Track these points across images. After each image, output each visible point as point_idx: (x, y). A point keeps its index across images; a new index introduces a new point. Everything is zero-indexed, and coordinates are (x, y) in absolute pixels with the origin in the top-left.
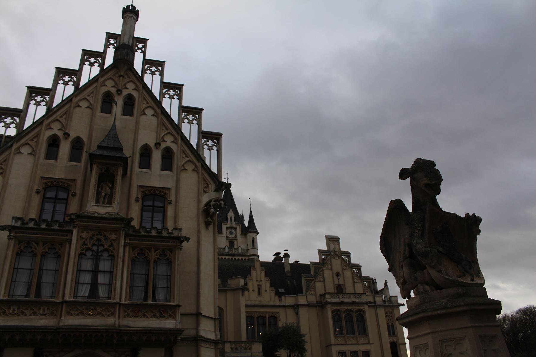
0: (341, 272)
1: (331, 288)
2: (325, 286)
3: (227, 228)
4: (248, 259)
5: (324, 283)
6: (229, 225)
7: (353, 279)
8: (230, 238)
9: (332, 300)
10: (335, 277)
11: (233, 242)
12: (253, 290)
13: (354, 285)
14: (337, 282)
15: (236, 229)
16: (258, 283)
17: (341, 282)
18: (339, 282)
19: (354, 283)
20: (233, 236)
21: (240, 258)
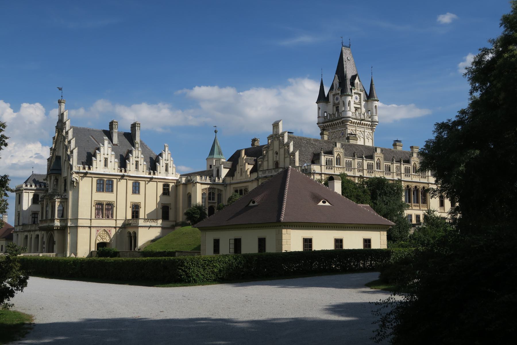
0: (278, 151)
1: (271, 165)
2: (268, 164)
3: (334, 95)
4: (342, 122)
5: (268, 162)
6: (334, 92)
7: (285, 154)
8: (336, 103)
9: (263, 176)
10: (275, 155)
11: (338, 107)
12: (239, 173)
13: (284, 160)
14: (275, 160)
15: (339, 93)
16: (241, 168)
17: (277, 160)
18: (276, 159)
19: (285, 158)
20: (338, 102)
21: (336, 122)
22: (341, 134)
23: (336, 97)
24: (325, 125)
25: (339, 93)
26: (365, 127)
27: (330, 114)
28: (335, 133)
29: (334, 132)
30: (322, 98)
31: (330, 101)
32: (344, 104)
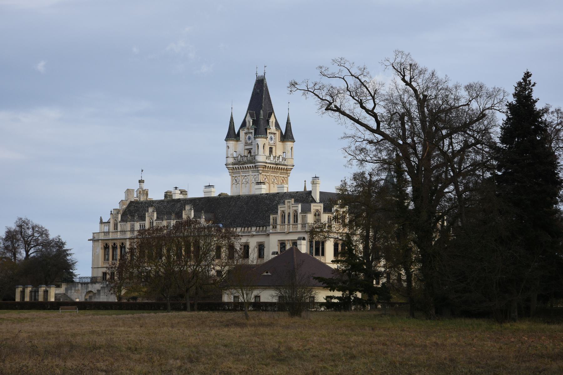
3: (246, 133)
4: (255, 166)
15: (252, 133)
20: (250, 141)
21: (249, 165)
22: (253, 180)
23: (248, 136)
24: (234, 166)
25: (252, 133)
26: (280, 171)
27: (241, 155)
28: (246, 177)
29: (246, 176)
30: (232, 135)
31: (241, 140)
32: (258, 146)
